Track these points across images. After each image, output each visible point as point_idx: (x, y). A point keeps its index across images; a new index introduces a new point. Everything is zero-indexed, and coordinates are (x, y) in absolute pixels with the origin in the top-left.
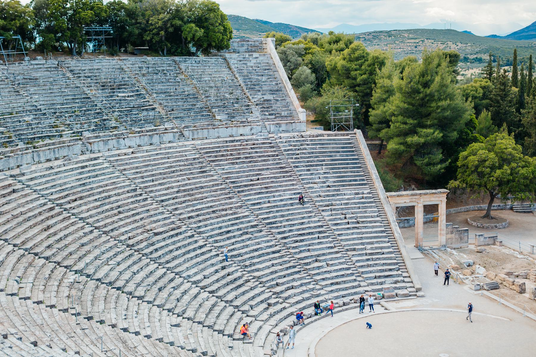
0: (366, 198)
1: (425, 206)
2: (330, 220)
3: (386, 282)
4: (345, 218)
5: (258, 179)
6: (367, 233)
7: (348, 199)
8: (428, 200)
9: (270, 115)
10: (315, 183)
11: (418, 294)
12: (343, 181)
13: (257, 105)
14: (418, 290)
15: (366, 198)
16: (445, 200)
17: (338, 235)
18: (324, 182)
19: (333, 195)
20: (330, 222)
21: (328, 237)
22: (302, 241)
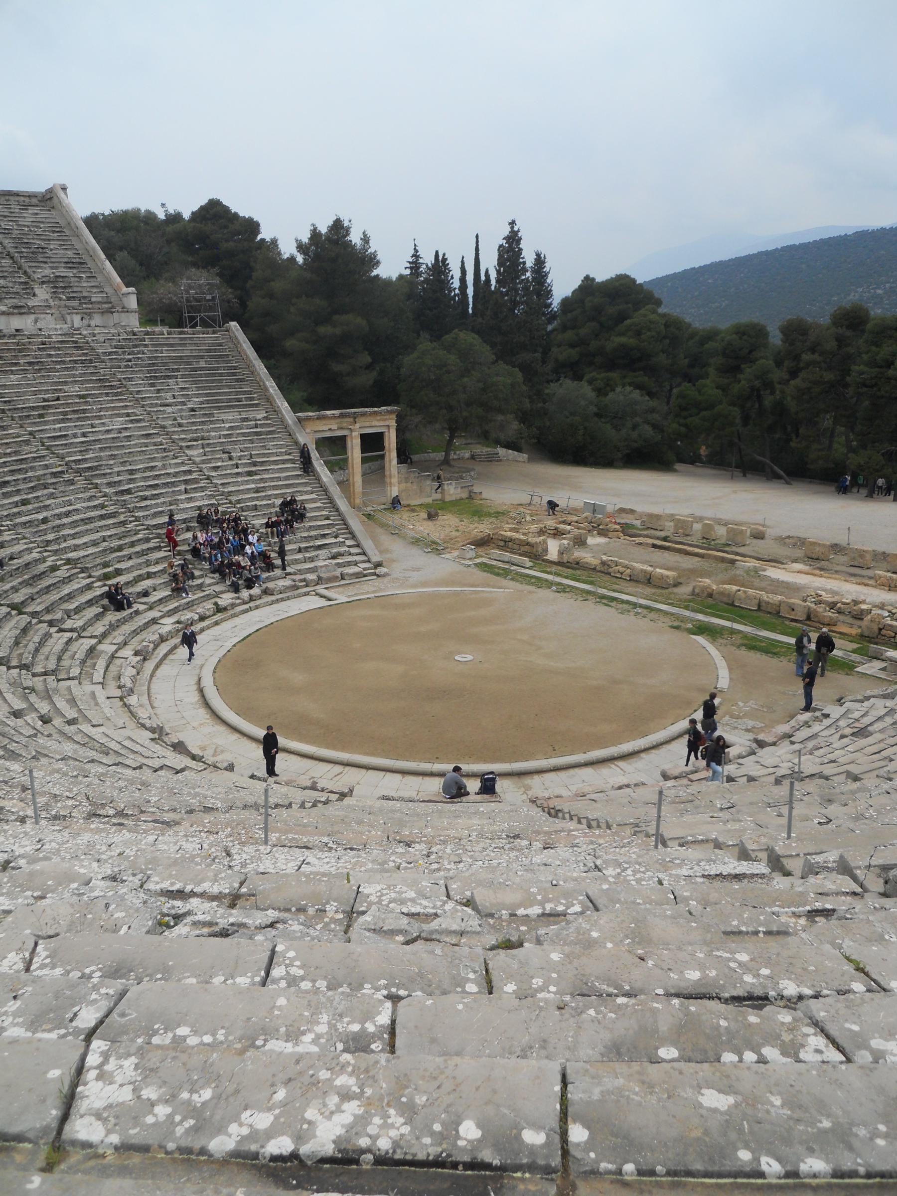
0: (262, 426)
1: (363, 437)
2: (203, 462)
3: (321, 557)
4: (231, 458)
5: (58, 399)
6: (272, 479)
7: (231, 428)
8: (367, 424)
9: (69, 299)
10: (167, 405)
11: (379, 570)
12: (217, 401)
13: (43, 283)
14: (378, 565)
15: (262, 426)
16: (393, 423)
17: (222, 484)
18: (183, 403)
19: (203, 423)
20: (204, 466)
21: (203, 489)
22: (154, 497)
